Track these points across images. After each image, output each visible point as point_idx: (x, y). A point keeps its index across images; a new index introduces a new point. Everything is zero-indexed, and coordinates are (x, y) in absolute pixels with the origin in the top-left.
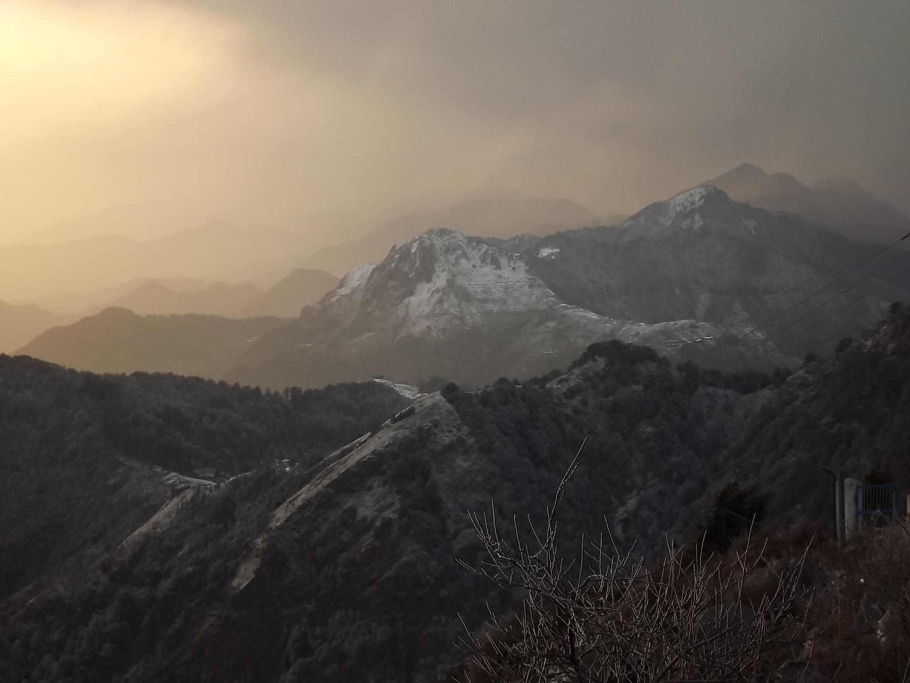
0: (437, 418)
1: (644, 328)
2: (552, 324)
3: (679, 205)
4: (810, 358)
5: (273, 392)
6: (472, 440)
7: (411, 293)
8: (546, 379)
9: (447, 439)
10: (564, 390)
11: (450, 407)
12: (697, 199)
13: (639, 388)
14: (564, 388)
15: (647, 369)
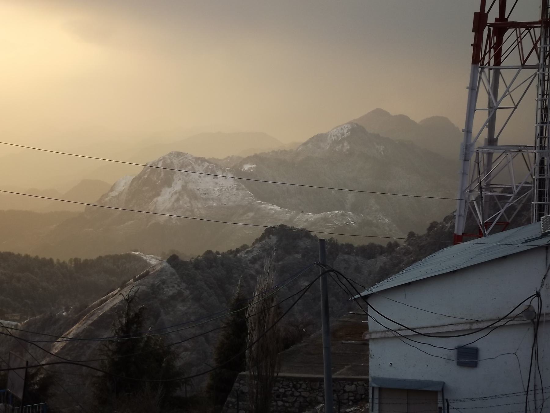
0: (164, 278)
1: (311, 216)
2: (251, 214)
3: (334, 136)
4: (411, 235)
5: (61, 261)
6: (188, 292)
7: (158, 194)
8: (238, 251)
9: (170, 292)
10: (250, 258)
11: (173, 270)
12: (345, 131)
13: (299, 256)
14: (250, 257)
15: (303, 243)
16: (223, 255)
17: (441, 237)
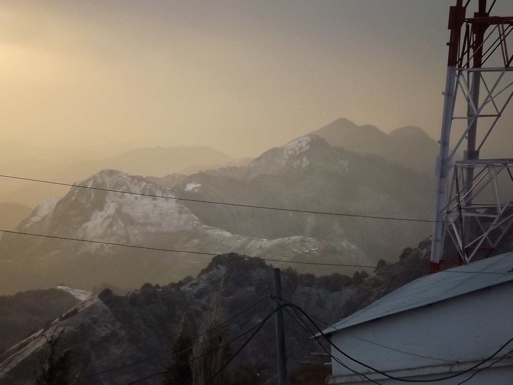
0: (95, 316)
1: (266, 243)
2: (196, 241)
3: (291, 150)
4: (382, 263)
6: (122, 333)
7: (88, 219)
8: (181, 284)
9: (103, 332)
10: (195, 292)
11: (105, 307)
12: (304, 145)
14: (195, 290)
16: (164, 288)
17: (415, 265)
